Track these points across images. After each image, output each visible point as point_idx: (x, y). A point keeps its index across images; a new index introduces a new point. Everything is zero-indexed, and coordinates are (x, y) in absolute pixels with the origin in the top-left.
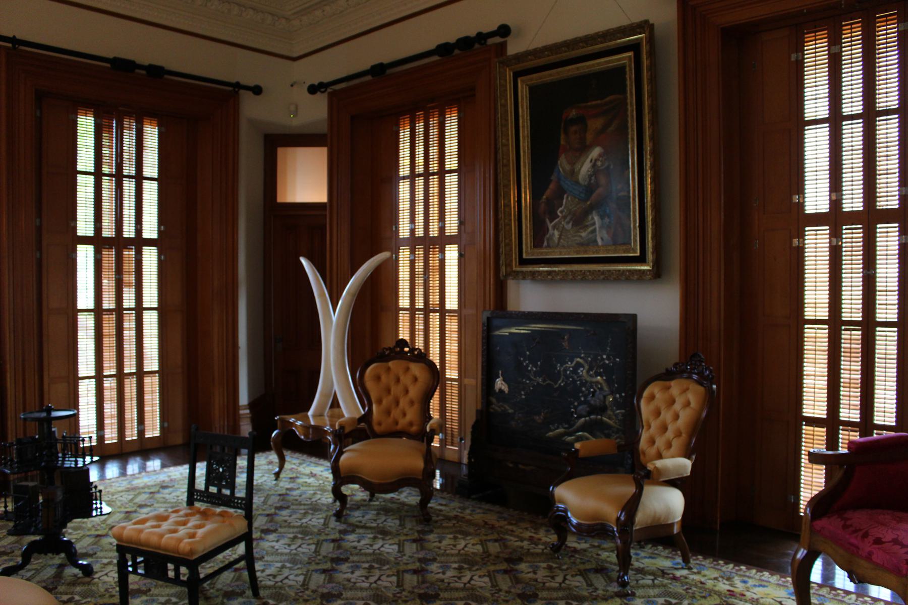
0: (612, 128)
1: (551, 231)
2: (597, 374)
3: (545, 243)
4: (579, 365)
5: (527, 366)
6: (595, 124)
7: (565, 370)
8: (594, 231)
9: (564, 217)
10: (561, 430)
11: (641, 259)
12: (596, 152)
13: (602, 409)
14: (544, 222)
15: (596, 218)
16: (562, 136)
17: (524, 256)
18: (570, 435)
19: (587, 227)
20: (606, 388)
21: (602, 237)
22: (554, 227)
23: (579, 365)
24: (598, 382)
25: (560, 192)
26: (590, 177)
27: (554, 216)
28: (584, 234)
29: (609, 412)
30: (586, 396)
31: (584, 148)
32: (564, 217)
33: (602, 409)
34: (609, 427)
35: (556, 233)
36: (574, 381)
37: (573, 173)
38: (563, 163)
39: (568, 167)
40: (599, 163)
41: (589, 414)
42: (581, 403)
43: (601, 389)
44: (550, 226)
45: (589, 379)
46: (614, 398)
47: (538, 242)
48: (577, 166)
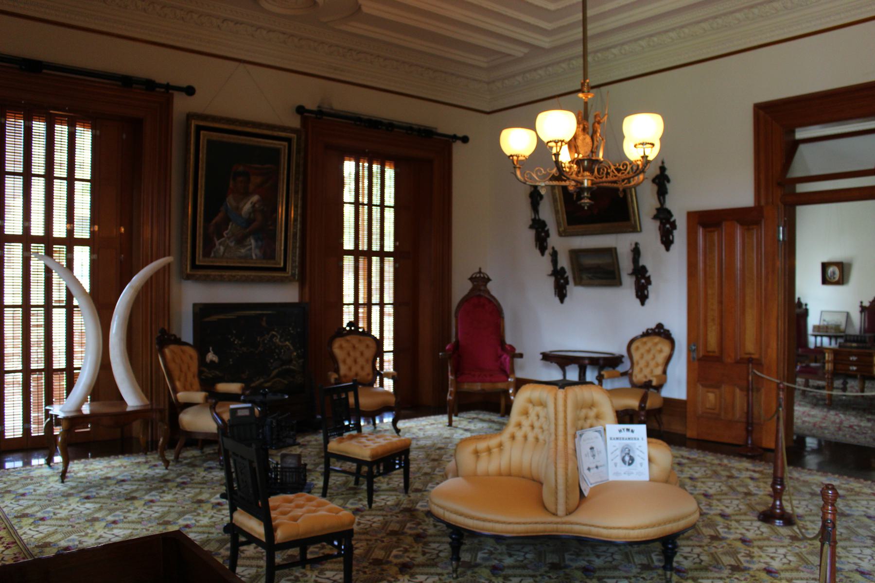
2: (286, 340)
3: (212, 255)
4: (274, 336)
8: (251, 249)
9: (229, 238)
10: (262, 380)
11: (284, 269)
12: (255, 198)
13: (290, 361)
15: (253, 241)
17: (197, 263)
19: (245, 246)
20: (291, 348)
21: (255, 253)
22: (220, 244)
25: (227, 221)
26: (250, 214)
27: (221, 236)
28: (243, 251)
29: (294, 362)
31: (247, 194)
32: (229, 238)
35: (222, 248)
37: (238, 209)
38: (230, 201)
40: (257, 206)
44: (217, 243)
47: (206, 254)
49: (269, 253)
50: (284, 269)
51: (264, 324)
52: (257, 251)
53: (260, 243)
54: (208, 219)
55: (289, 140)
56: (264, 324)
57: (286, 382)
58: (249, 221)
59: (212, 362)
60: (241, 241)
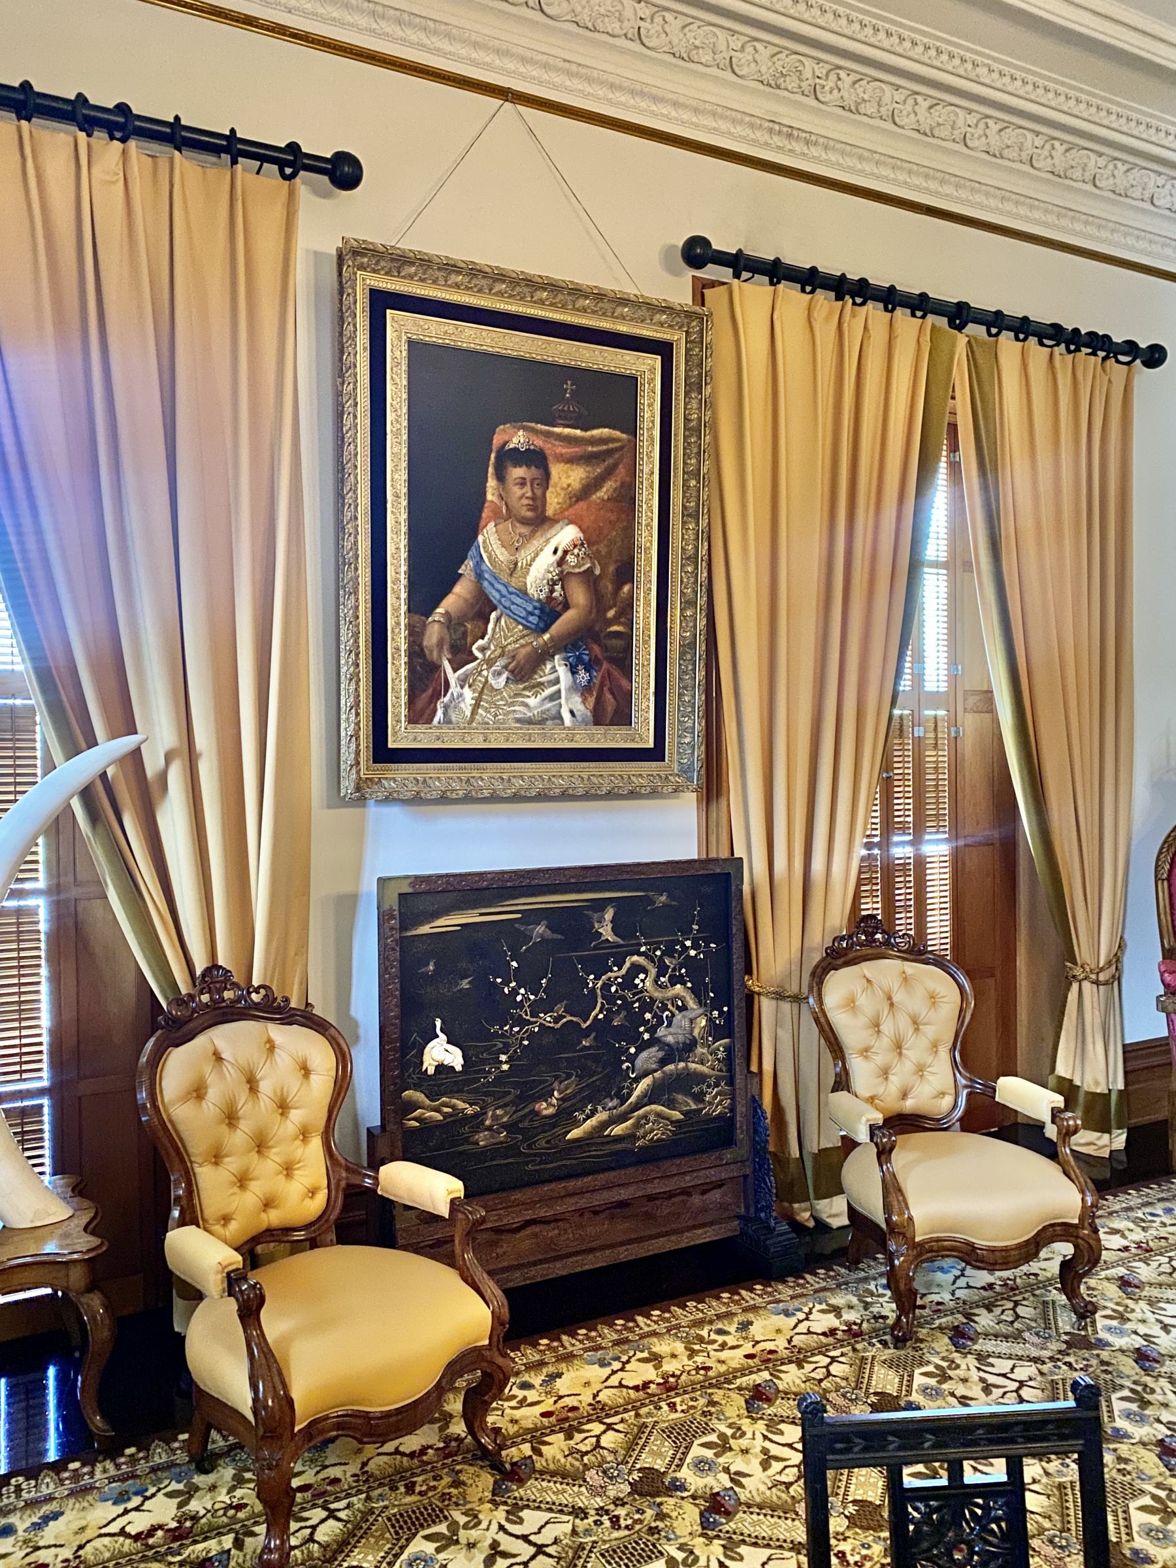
0: (603, 493)
1: (454, 689)
2: (673, 981)
3: (439, 714)
4: (637, 969)
5: (514, 992)
6: (567, 477)
7: (606, 986)
10: (602, 1116)
12: (567, 535)
13: (690, 1046)
14: (436, 667)
15: (563, 672)
16: (491, 483)
18: (623, 1118)
20: (691, 1004)
21: (573, 705)
22: (462, 682)
23: (637, 969)
24: (673, 1000)
27: (461, 655)
28: (532, 702)
29: (700, 1050)
30: (652, 1030)
33: (690, 1046)
34: (701, 1078)
35: (468, 694)
36: (627, 1005)
38: (491, 540)
39: (502, 555)
40: (570, 558)
41: (663, 1062)
42: (643, 1046)
43: (683, 1008)
44: (453, 677)
45: (657, 994)
46: (710, 1020)
47: (419, 714)
48: (524, 556)
49: (612, 708)
50: (656, 754)
51: (606, 932)
52: (577, 703)
53: (583, 676)
54: (424, 599)
55: (663, 349)
56: (606, 932)
57: (677, 1115)
58: (548, 612)
59: (441, 1068)
60: (524, 672)
